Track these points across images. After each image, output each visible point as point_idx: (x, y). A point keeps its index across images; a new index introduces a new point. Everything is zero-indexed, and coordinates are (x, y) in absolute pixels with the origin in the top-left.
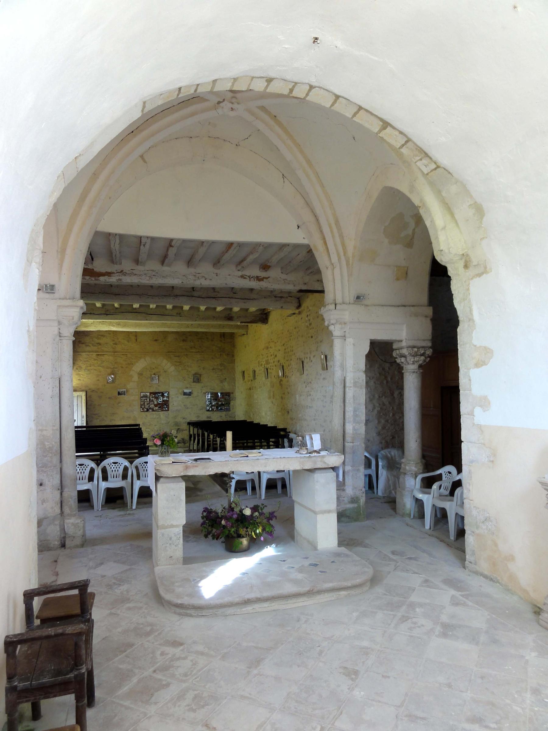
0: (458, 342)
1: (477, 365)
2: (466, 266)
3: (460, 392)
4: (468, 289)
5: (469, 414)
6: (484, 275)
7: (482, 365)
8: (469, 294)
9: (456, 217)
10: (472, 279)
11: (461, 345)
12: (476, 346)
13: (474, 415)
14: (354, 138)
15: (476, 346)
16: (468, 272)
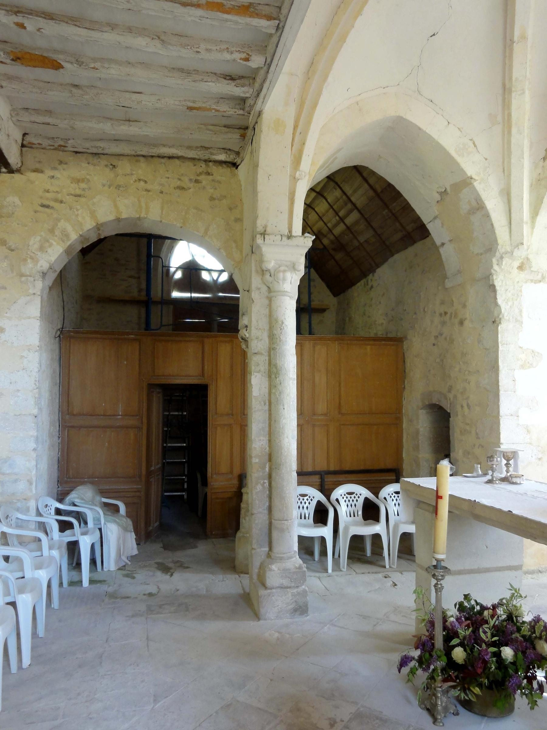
0: (499, 341)
1: (522, 367)
2: (521, 268)
3: (501, 392)
4: (521, 291)
5: (512, 415)
6: (542, 283)
7: (529, 367)
8: (521, 295)
9: (539, 219)
10: (526, 282)
11: (504, 344)
12: (522, 348)
13: (518, 416)
14: (434, 35)
15: (522, 348)
16: (522, 274)
